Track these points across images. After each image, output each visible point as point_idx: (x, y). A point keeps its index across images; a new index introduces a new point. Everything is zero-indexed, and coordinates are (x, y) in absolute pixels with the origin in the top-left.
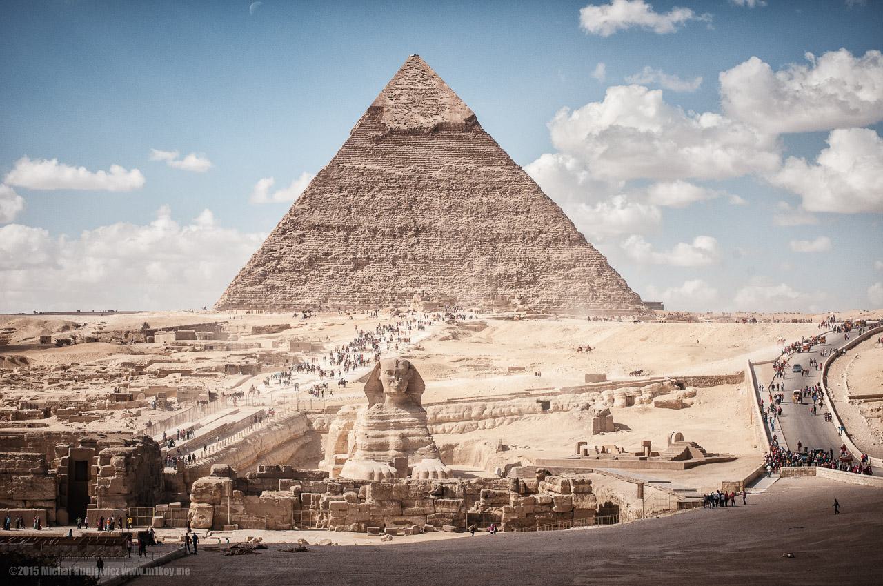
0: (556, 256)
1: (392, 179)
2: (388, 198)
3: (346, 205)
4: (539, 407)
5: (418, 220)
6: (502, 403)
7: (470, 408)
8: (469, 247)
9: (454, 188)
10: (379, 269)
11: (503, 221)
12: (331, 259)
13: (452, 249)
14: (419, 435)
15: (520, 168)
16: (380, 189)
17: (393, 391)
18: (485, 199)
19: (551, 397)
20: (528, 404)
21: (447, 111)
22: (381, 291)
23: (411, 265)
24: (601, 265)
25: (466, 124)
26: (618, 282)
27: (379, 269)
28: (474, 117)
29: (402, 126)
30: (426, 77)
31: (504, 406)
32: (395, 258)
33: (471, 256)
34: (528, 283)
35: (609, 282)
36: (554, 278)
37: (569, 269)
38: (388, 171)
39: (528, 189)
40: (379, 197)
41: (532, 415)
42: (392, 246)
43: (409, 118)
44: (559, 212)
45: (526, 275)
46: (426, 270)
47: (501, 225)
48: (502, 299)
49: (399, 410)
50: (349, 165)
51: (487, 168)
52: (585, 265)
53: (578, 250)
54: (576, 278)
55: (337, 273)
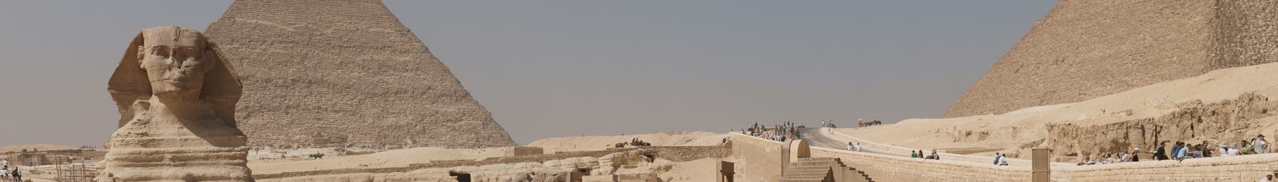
18: (375, 57)
32: (288, 107)
33: (363, 107)
34: (418, 133)
36: (443, 130)
40: (271, 50)
44: (447, 71)
47: (391, 80)
49: (185, 130)
53: (463, 106)
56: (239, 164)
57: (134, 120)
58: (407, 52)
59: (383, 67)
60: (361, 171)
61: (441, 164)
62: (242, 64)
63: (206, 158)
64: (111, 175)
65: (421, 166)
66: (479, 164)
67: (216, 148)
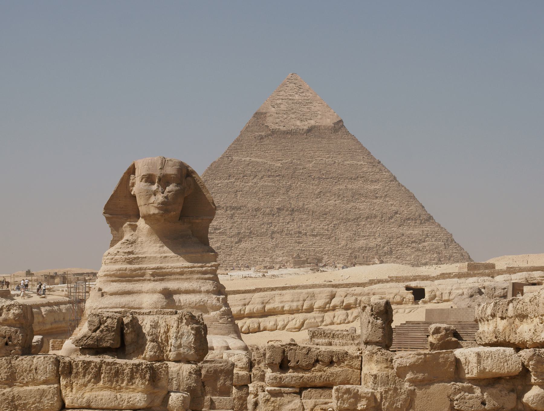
0: (409, 232)
1: (272, 169)
2: (270, 184)
3: (233, 190)
4: (410, 296)
5: (293, 203)
6: (358, 290)
7: (313, 296)
8: (336, 224)
9: (324, 177)
10: (260, 242)
11: (364, 203)
12: (220, 233)
13: (321, 226)
14: (200, 292)
15: (379, 162)
16: (262, 178)
17: (153, 211)
18: (350, 186)
19: (425, 282)
20: (395, 291)
21: (319, 117)
22: (261, 259)
23: (288, 239)
24: (447, 240)
25: (335, 127)
26: (462, 255)
27: (260, 242)
28: (341, 121)
29: (282, 128)
30: (302, 90)
31: (360, 295)
32: (273, 232)
33: (338, 232)
35: (454, 255)
36: (408, 250)
37: (419, 243)
38: (269, 162)
39: (386, 178)
40: (261, 183)
41: (399, 306)
42: (271, 223)
43: (287, 122)
44: (413, 197)
45: (383, 247)
46: (299, 243)
47: (363, 207)
48: (364, 258)
49: (166, 248)
50: (237, 158)
51: (352, 162)
52: (433, 240)
53: (427, 228)
54: (427, 251)
55: (224, 245)
56: (209, 279)
57: (123, 240)
58: (377, 181)
59: (356, 195)
60: (325, 286)
61: (398, 280)
62: (236, 196)
63: (182, 273)
64: (100, 290)
65: (379, 281)
66: (433, 279)
67: (190, 264)
